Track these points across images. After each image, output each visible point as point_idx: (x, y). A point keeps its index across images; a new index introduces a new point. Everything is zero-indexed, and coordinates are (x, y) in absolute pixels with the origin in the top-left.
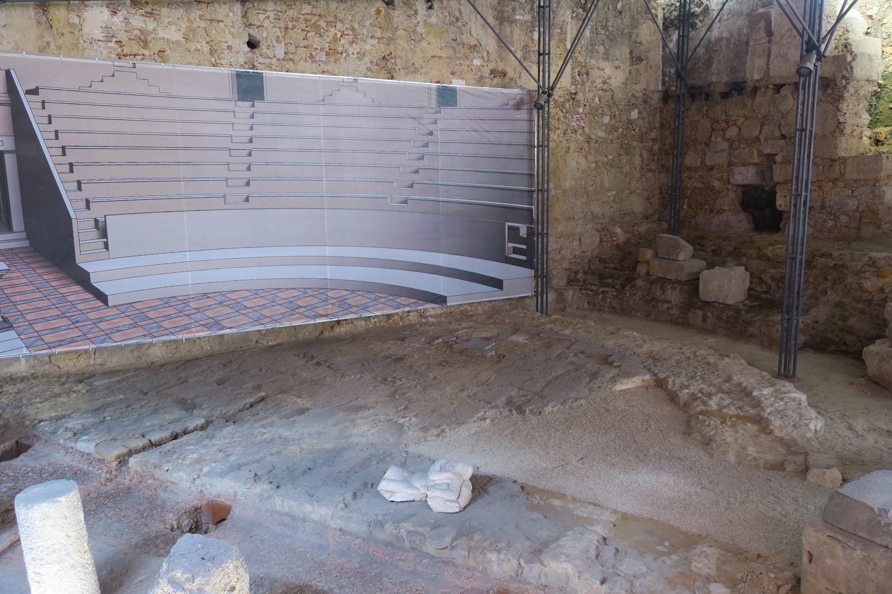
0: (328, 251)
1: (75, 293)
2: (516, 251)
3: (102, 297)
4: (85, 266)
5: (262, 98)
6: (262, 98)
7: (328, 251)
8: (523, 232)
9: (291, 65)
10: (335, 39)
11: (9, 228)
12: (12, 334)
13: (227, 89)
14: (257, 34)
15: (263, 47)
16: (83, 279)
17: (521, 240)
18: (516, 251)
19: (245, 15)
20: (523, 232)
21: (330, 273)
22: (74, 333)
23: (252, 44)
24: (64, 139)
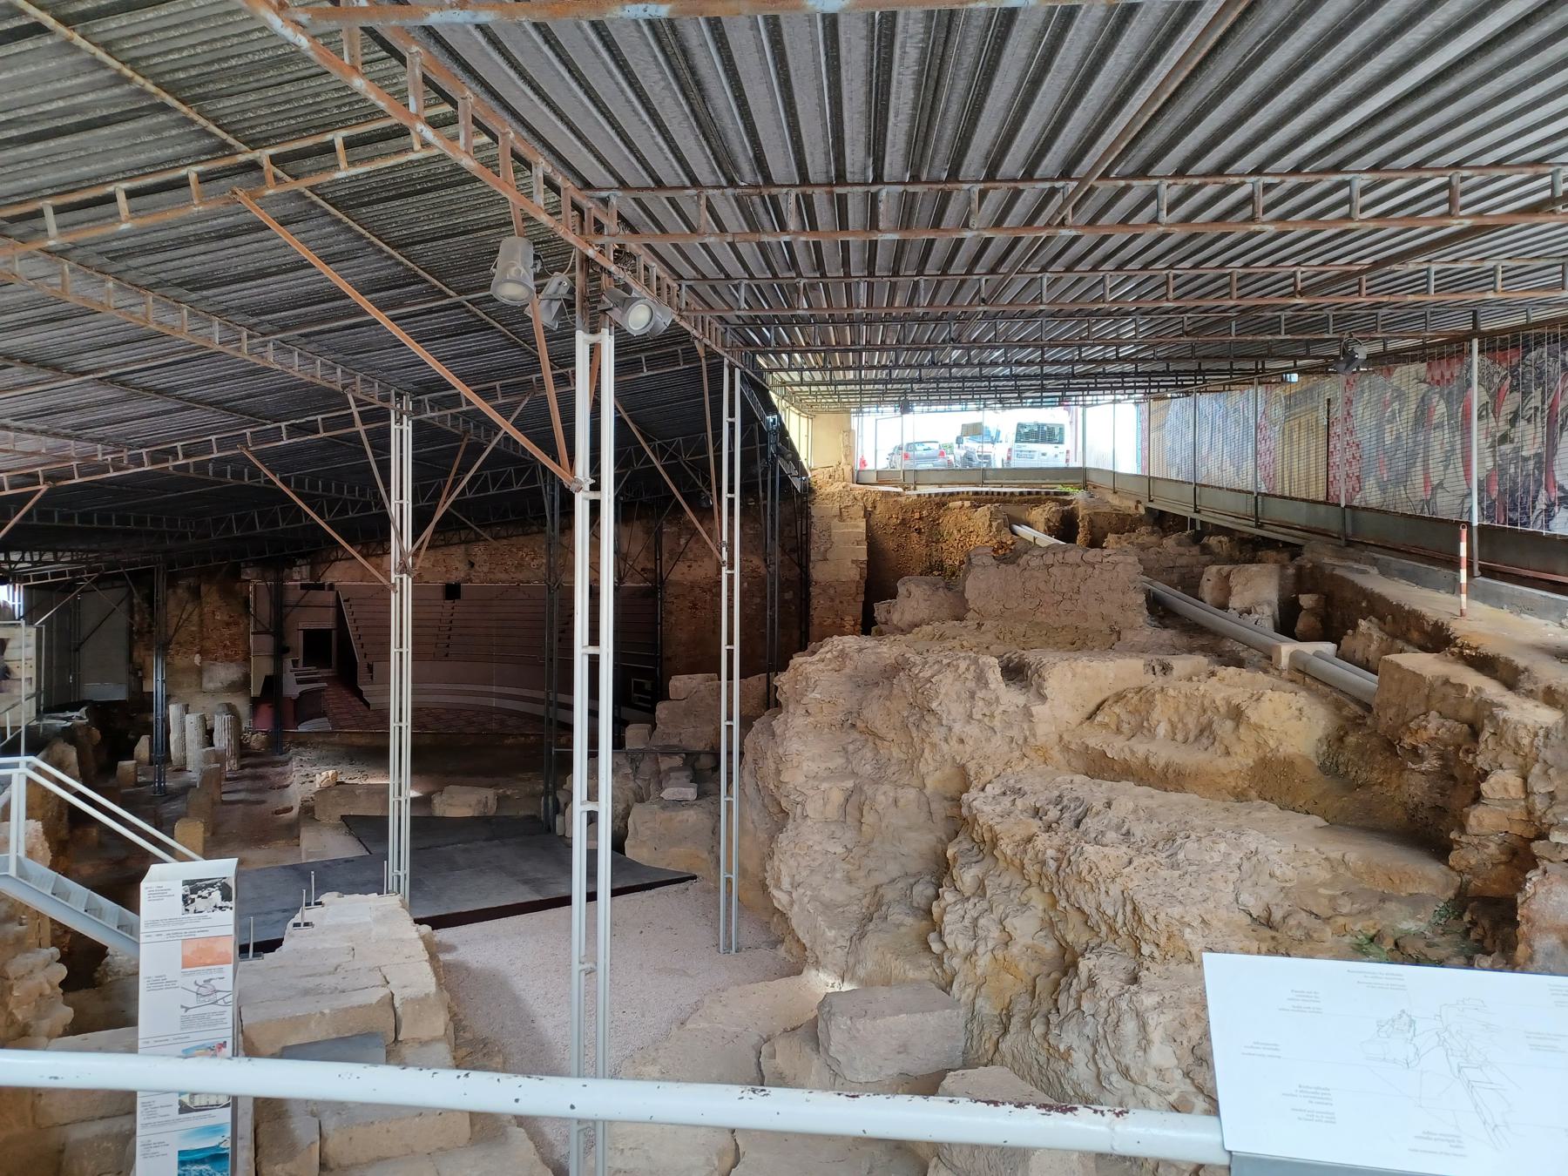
0: (494, 689)
1: (354, 700)
2: (641, 700)
3: (367, 705)
4: (362, 688)
5: (459, 597)
6: (459, 597)
7: (494, 689)
8: (648, 686)
9: (492, 576)
10: (522, 558)
11: (330, 667)
12: (326, 719)
13: (441, 595)
14: (473, 559)
15: (476, 567)
16: (359, 694)
17: (646, 693)
18: (641, 700)
19: (466, 550)
20: (648, 686)
21: (494, 702)
22: (353, 722)
23: (472, 565)
24: (359, 623)
